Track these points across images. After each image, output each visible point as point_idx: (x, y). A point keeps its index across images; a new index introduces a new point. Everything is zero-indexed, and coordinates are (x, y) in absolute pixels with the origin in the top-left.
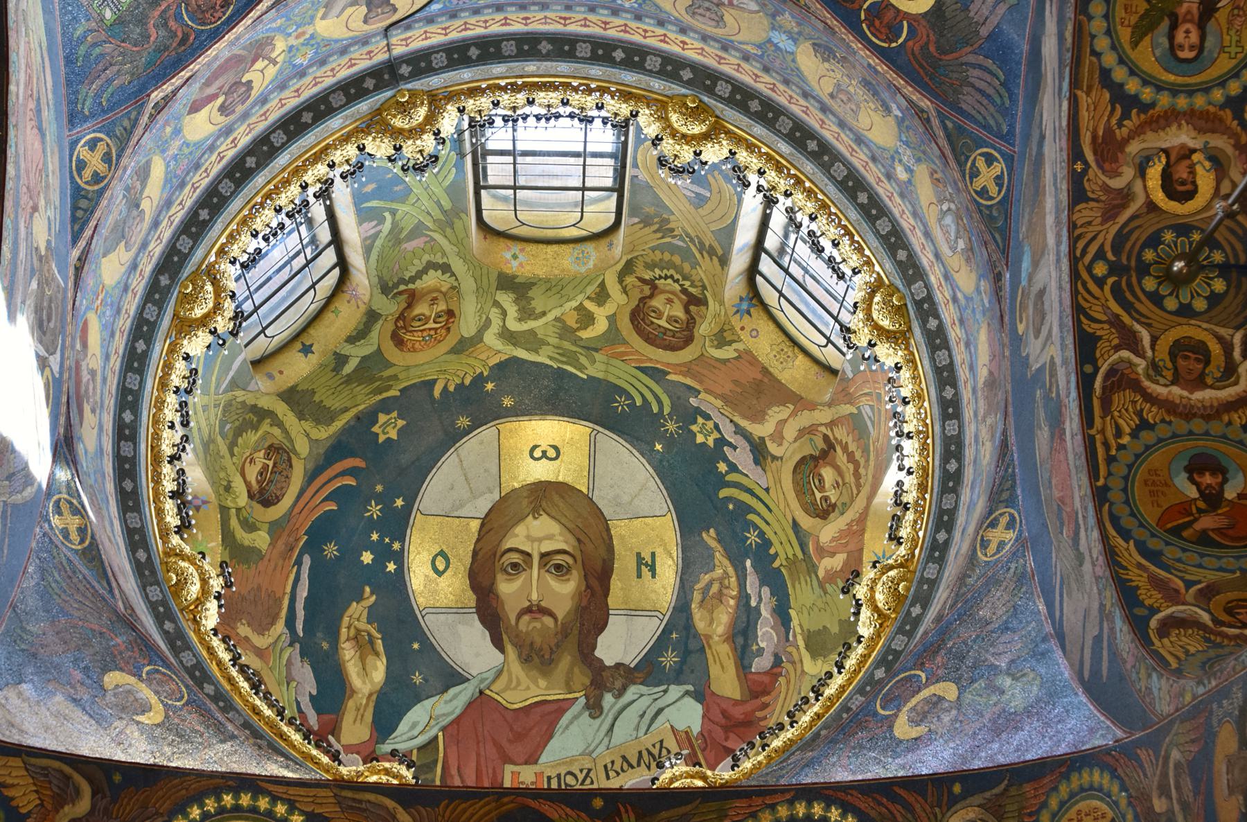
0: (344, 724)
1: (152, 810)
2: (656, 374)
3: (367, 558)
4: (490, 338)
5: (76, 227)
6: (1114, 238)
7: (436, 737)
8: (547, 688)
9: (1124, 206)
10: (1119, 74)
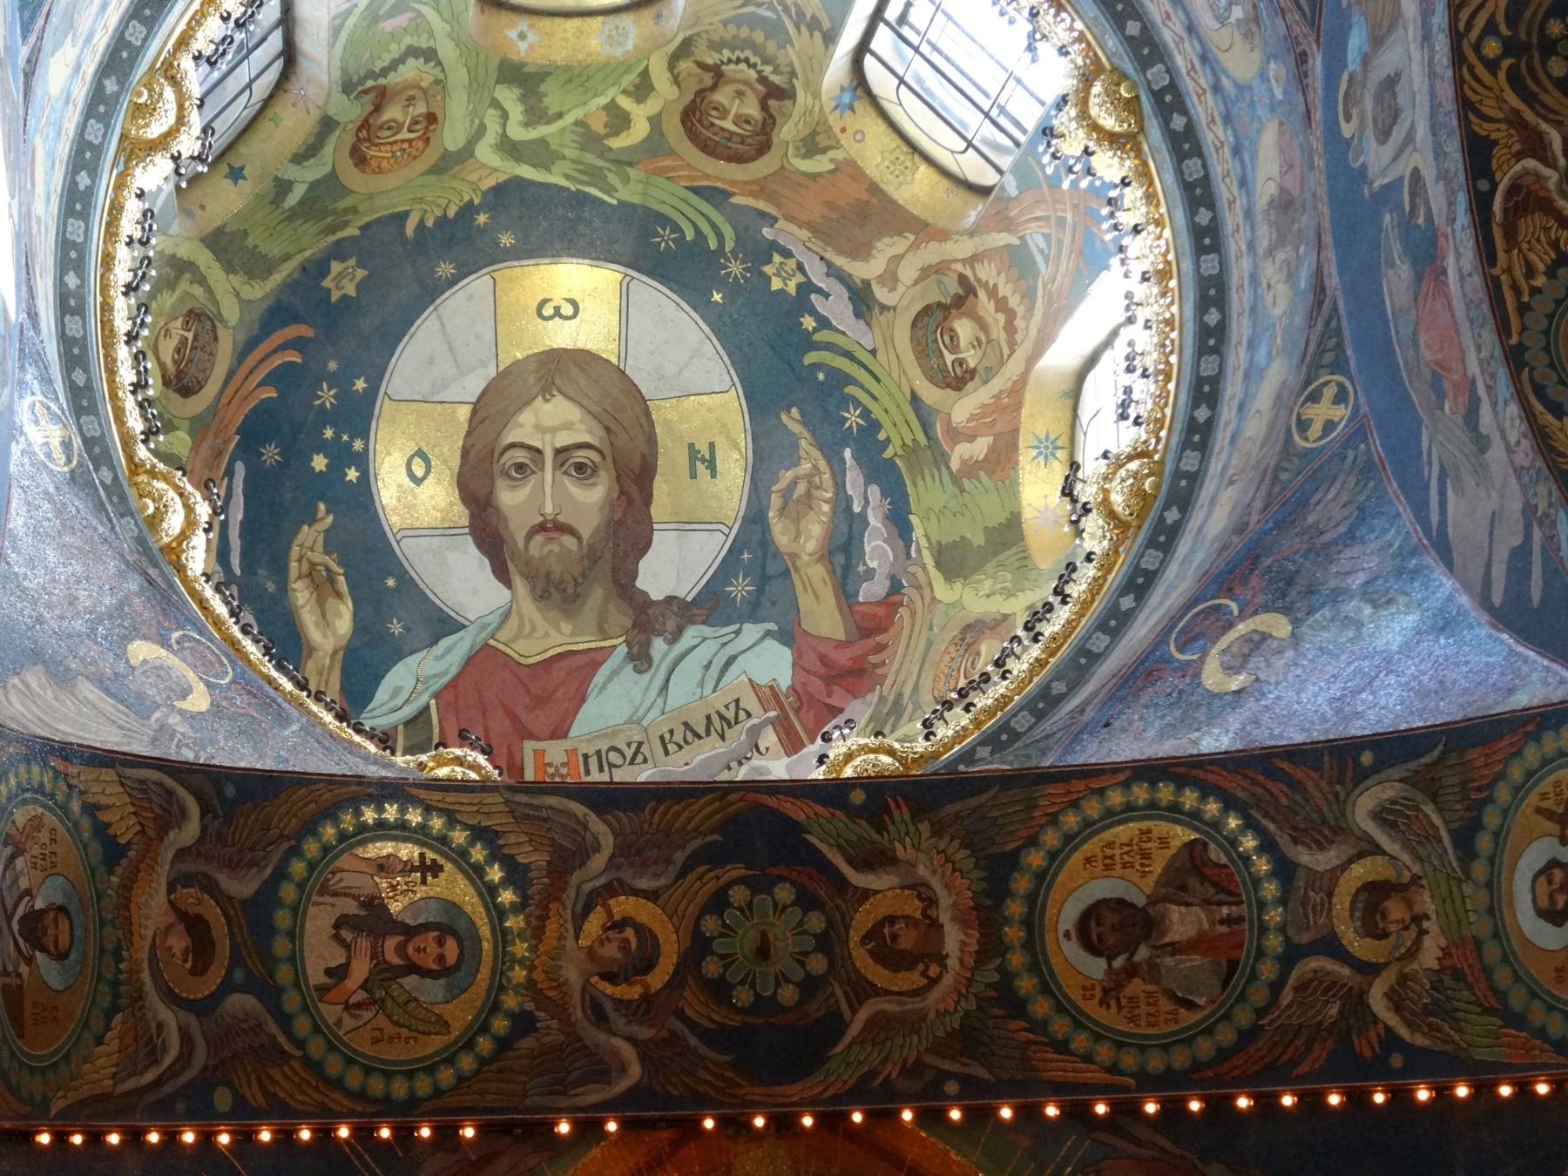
1: (275, 832)
2: (715, 196)
4: (485, 152)
7: (427, 707)
8: (572, 635)
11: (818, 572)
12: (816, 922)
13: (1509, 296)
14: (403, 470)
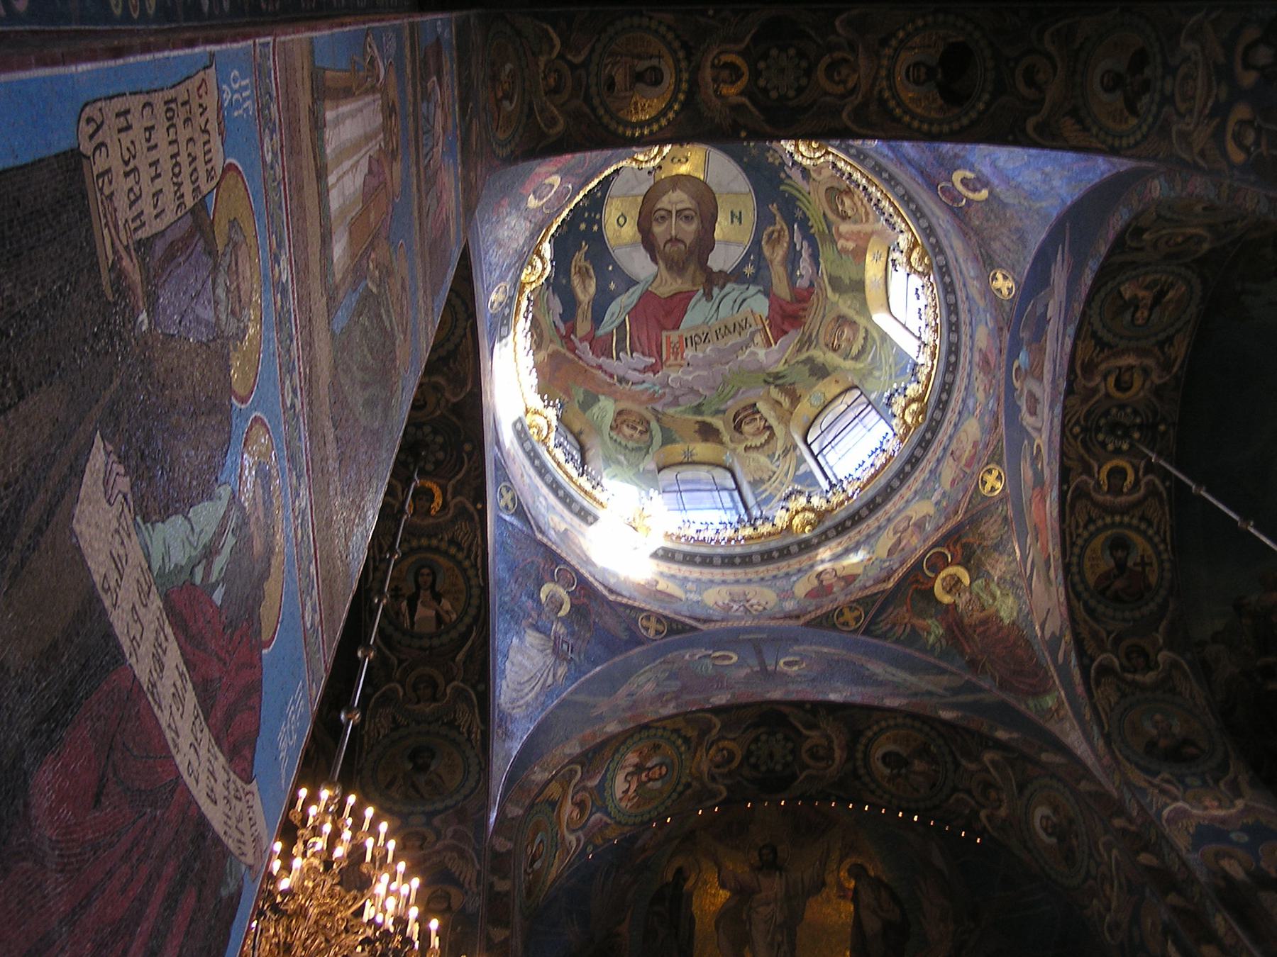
3: (583, 226)
10: (1102, 333)
12: (790, 745)
13: (1068, 538)
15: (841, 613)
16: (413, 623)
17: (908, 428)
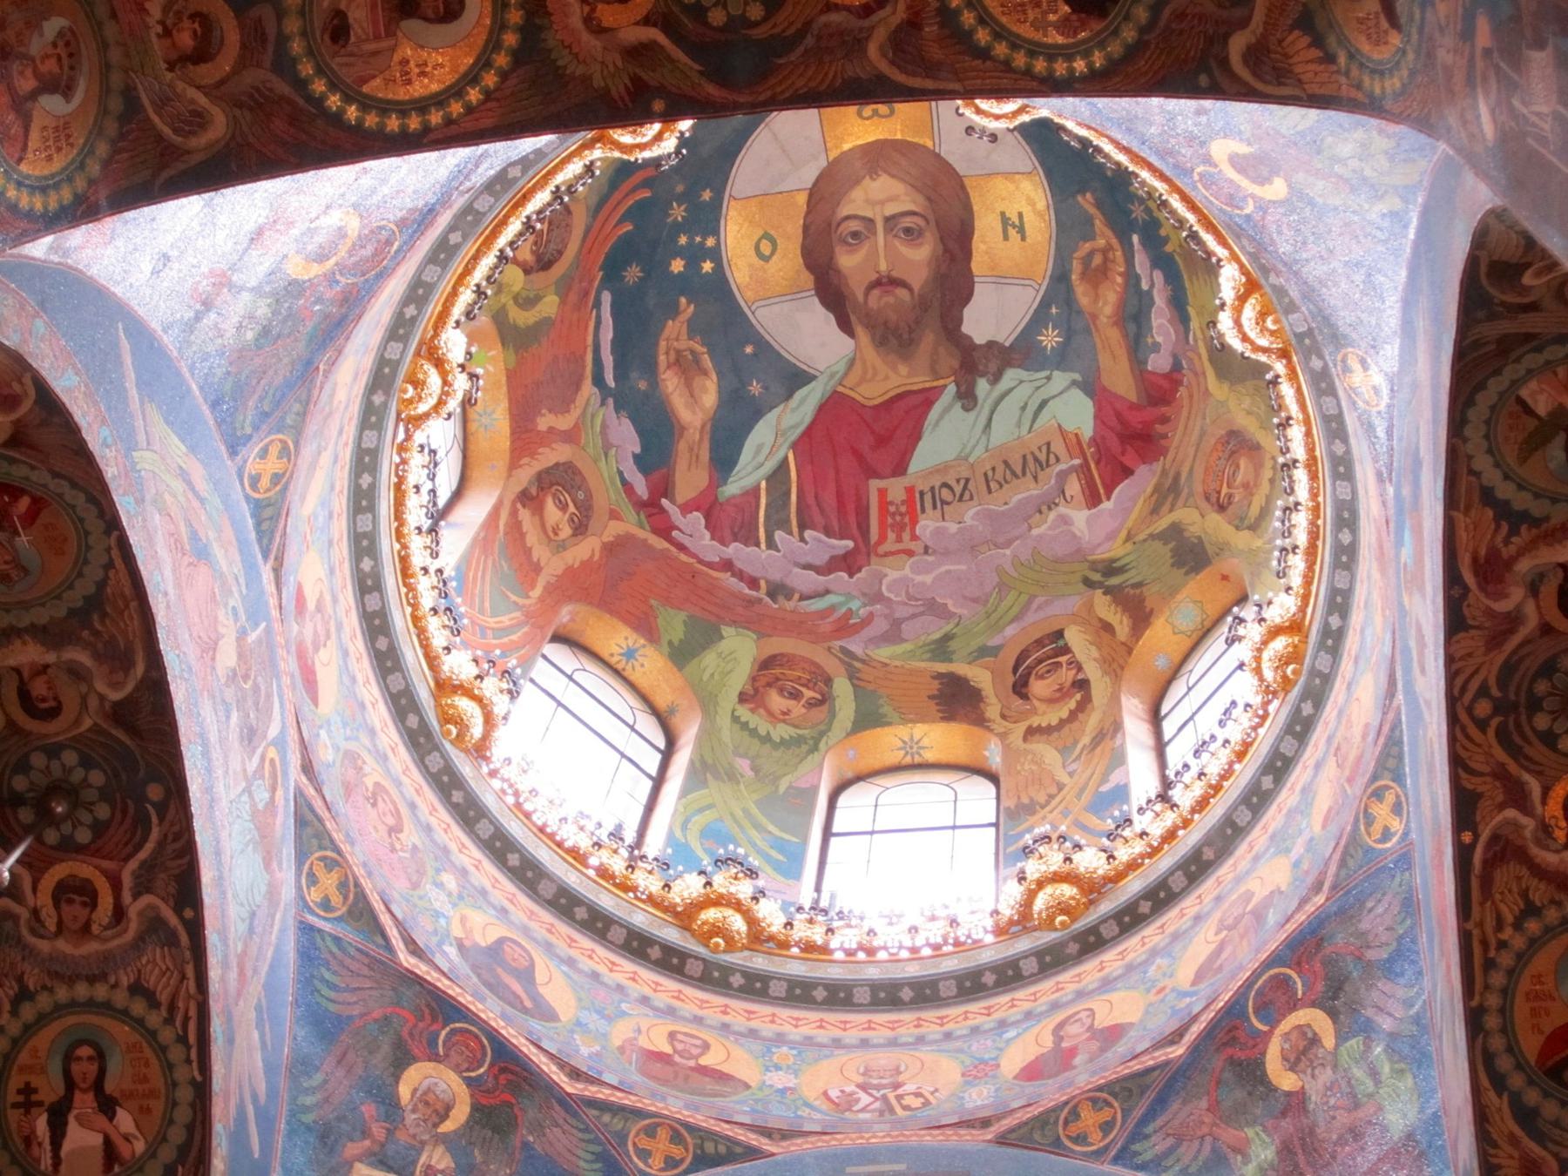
0: (678, 475)
3: (677, 266)
5: (265, 541)
6: (1500, 670)
8: (909, 376)
9: (1512, 631)
10: (1505, 491)
11: (1114, 335)
14: (753, 252)
15: (1075, 1114)
16: (57, 1162)
17: (1269, 692)
